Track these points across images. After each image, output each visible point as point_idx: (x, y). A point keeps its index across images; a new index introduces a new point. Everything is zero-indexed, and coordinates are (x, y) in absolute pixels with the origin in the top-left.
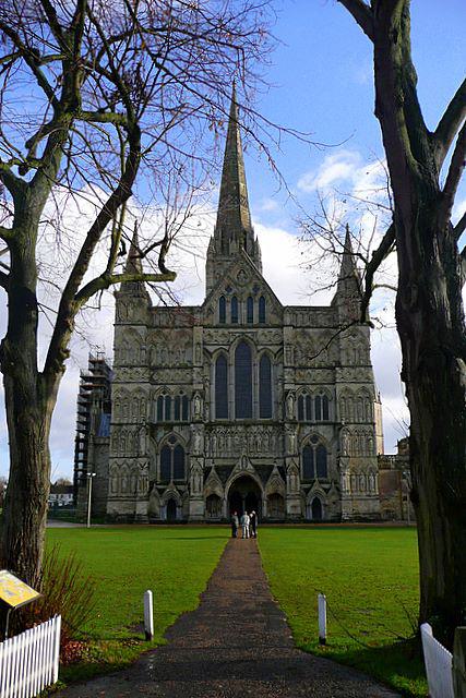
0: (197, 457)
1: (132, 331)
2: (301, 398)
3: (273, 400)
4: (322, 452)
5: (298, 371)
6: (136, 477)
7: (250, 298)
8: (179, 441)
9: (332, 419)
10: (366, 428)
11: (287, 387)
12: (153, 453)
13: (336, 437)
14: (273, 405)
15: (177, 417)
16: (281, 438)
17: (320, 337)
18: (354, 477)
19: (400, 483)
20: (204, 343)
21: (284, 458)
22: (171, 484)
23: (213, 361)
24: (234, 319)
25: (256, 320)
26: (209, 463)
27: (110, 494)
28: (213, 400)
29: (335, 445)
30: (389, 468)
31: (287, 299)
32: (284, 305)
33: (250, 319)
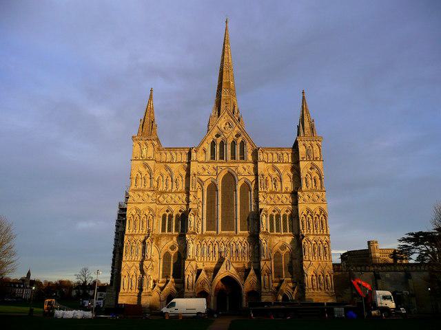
2: (271, 216)
10: (322, 238)
15: (176, 230)
18: (315, 278)
19: (352, 283)
20: (199, 174)
23: (205, 188)
24: (222, 158)
26: (200, 267)
28: (205, 217)
30: (342, 271)
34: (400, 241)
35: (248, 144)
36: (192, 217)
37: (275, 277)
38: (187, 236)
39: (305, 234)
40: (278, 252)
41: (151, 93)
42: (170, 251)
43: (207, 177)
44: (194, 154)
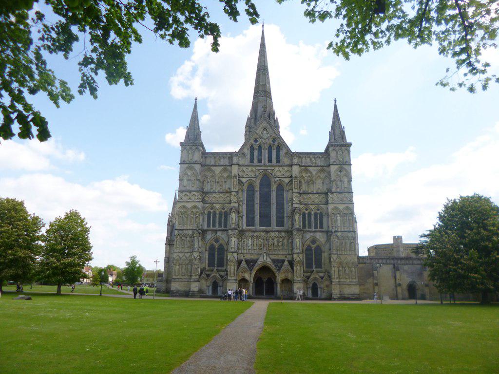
0: (233, 252)
1: (190, 168)
2: (304, 214)
4: (319, 251)
5: (302, 195)
6: (191, 265)
8: (221, 242)
9: (325, 228)
10: (350, 235)
11: (294, 206)
12: (203, 249)
13: (328, 240)
14: (285, 218)
15: (220, 225)
16: (290, 241)
17: (316, 174)
18: (341, 269)
19: (373, 273)
21: (292, 255)
22: (215, 270)
23: (245, 188)
24: (260, 161)
26: (241, 257)
27: (174, 277)
28: (245, 214)
29: (327, 246)
30: (365, 263)
31: (294, 149)
32: (293, 151)
33: (270, 161)
34: (421, 237)
35: (284, 148)
38: (230, 231)
39: (333, 230)
41: (196, 102)
43: (247, 179)
44: (235, 160)
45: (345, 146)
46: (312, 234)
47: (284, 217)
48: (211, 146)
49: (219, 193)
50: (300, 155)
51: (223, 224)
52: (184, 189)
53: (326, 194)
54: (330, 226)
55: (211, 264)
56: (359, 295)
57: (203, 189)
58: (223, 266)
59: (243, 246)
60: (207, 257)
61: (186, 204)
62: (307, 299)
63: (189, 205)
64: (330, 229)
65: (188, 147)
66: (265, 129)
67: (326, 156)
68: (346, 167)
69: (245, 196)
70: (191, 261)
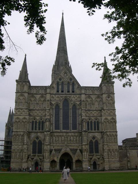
0: (47, 145)
3: (77, 123)
4: (97, 143)
7: (69, 83)
8: (40, 139)
9: (100, 130)
10: (114, 134)
11: (83, 118)
12: (29, 143)
14: (77, 125)
15: (39, 129)
16: (80, 138)
17: (95, 99)
18: (109, 153)
19: (127, 155)
23: (54, 107)
24: (62, 92)
25: (71, 91)
26: (52, 148)
28: (54, 123)
29: (102, 140)
31: (82, 84)
32: (82, 86)
33: (68, 92)
36: (48, 123)
37: (90, 153)
39: (105, 132)
40: (91, 140)
41: (26, 57)
42: (36, 140)
44: (48, 91)
45: (111, 83)
46: (93, 134)
47: (77, 125)
48: (34, 83)
49: (38, 110)
50: (86, 88)
51: (41, 128)
52: (18, 107)
53: (101, 111)
54: (103, 129)
55: (34, 152)
56: (119, 167)
57: (29, 108)
58: (41, 154)
59: (53, 141)
60: (32, 148)
61: (19, 117)
62: (91, 171)
63: (21, 117)
64: (103, 131)
65: (21, 83)
66: (65, 73)
67: (100, 89)
68: (111, 95)
69: (54, 112)
70: (22, 150)
